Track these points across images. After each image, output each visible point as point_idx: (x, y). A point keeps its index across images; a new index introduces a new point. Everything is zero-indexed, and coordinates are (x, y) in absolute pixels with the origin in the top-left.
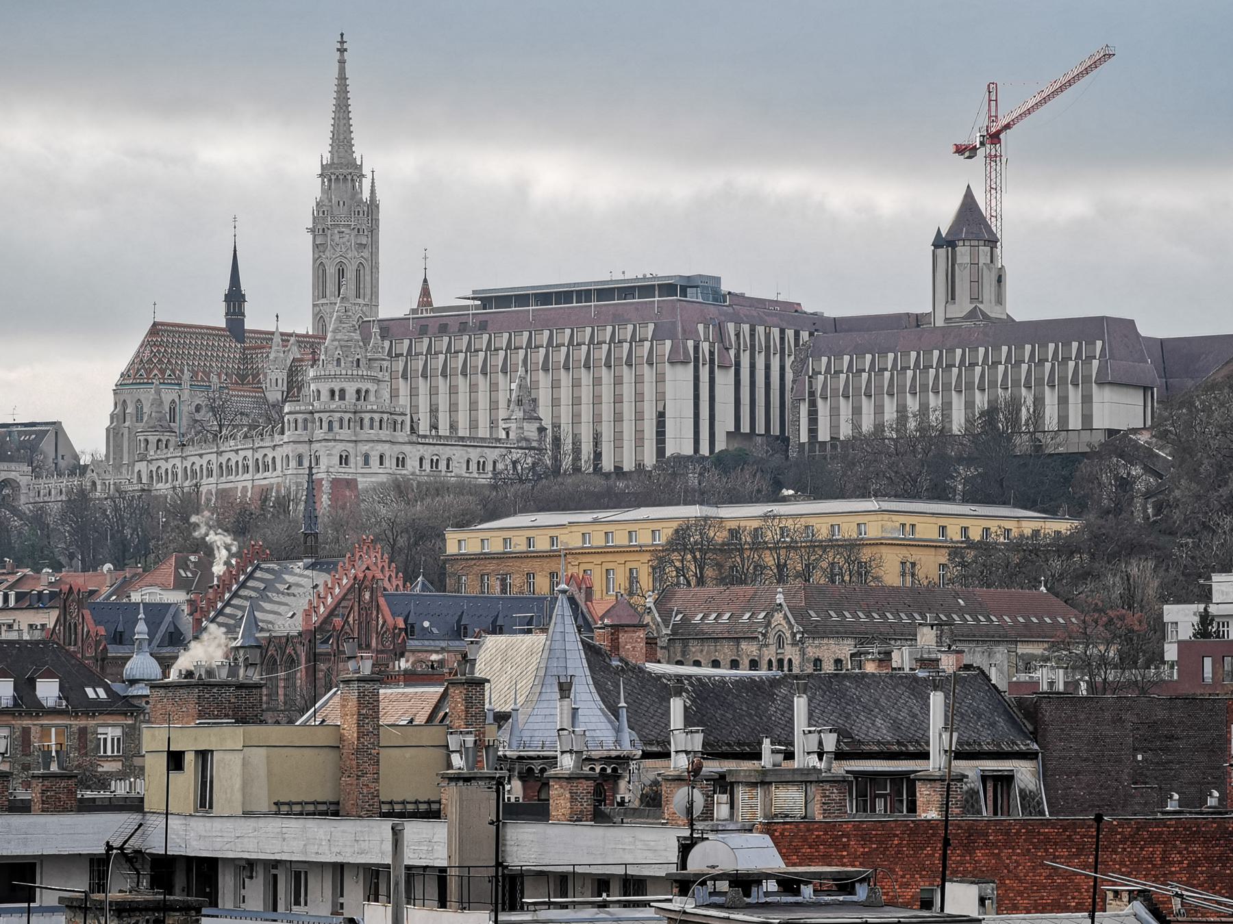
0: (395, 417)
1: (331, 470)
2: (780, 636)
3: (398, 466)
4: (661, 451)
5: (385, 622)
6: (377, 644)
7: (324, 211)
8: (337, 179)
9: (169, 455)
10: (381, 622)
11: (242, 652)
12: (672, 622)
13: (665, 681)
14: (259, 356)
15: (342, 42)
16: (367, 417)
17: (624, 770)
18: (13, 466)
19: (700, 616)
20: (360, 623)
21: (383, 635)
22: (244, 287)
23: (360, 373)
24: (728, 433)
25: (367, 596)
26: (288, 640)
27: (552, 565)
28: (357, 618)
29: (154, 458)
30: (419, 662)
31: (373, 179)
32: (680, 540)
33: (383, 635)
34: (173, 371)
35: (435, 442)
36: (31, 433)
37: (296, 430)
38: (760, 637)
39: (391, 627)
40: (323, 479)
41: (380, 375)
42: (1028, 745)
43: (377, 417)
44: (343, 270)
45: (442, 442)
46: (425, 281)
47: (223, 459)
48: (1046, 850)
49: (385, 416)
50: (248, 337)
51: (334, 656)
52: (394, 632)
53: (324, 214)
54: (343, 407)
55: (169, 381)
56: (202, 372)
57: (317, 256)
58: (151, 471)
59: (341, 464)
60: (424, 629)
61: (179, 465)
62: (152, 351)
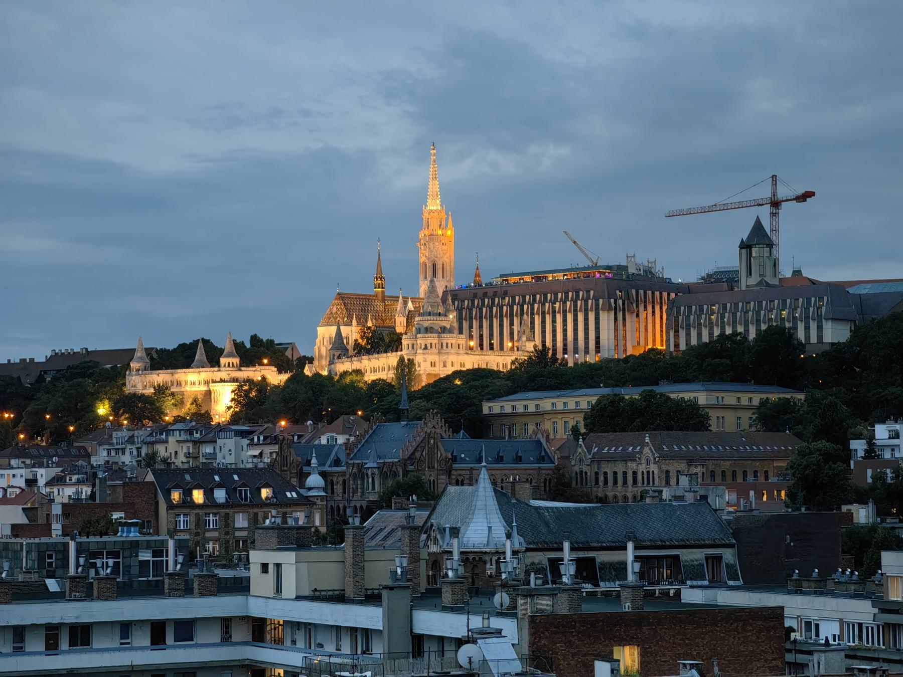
2: (647, 459)
5: (441, 455)
10: (439, 455)
11: (370, 470)
19: (607, 448)
25: (432, 441)
26: (393, 465)
27: (537, 419)
38: (637, 459)
48: (681, 626)
59: (432, 366)
60: (462, 458)
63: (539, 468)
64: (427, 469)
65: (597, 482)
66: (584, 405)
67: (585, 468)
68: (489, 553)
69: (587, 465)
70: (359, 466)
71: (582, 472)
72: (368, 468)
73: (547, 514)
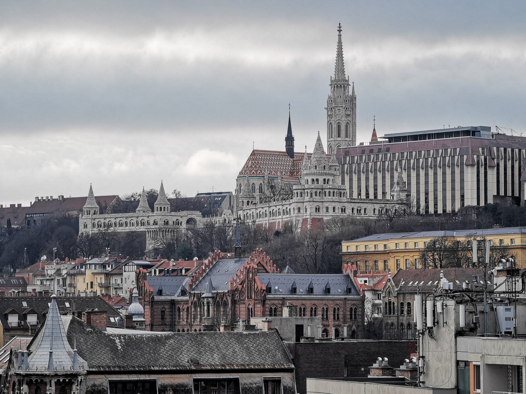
0: (341, 191)
1: (312, 214)
3: (342, 212)
4: (463, 204)
5: (257, 287)
6: (255, 297)
7: (331, 100)
8: (337, 87)
9: (251, 208)
10: (256, 287)
11: (205, 300)
12: (400, 285)
13: (111, 337)
14: (299, 164)
15: (340, 27)
16: (327, 191)
17: (75, 380)
18: (193, 212)
19: (412, 282)
20: (248, 287)
21: (257, 292)
22: (294, 134)
23: (325, 172)
24: (494, 196)
26: (224, 294)
27: (385, 257)
28: (247, 285)
29: (245, 209)
30: (272, 304)
31: (353, 86)
32: (431, 248)
33: (257, 292)
34: (261, 171)
35: (359, 201)
36: (219, 197)
37: (297, 197)
39: (260, 289)
40: (308, 218)
41: (335, 173)
42: (289, 365)
43: (332, 191)
44: (340, 125)
45: (362, 201)
46: (374, 130)
47: (271, 210)
49: (336, 191)
50: (295, 156)
51: (239, 302)
52: (261, 291)
53: (332, 102)
54: (317, 186)
55: (259, 175)
56: (274, 171)
57: (329, 120)
58: (245, 215)
59: (316, 211)
60: (275, 290)
61: (254, 212)
62: (252, 162)
63: (345, 298)
64: (246, 299)
65: (402, 312)
66: (421, 246)
67: (393, 300)
68: (49, 376)
69: (395, 297)
70: (198, 296)
71: (390, 303)
72: (203, 298)
73: (119, 341)
